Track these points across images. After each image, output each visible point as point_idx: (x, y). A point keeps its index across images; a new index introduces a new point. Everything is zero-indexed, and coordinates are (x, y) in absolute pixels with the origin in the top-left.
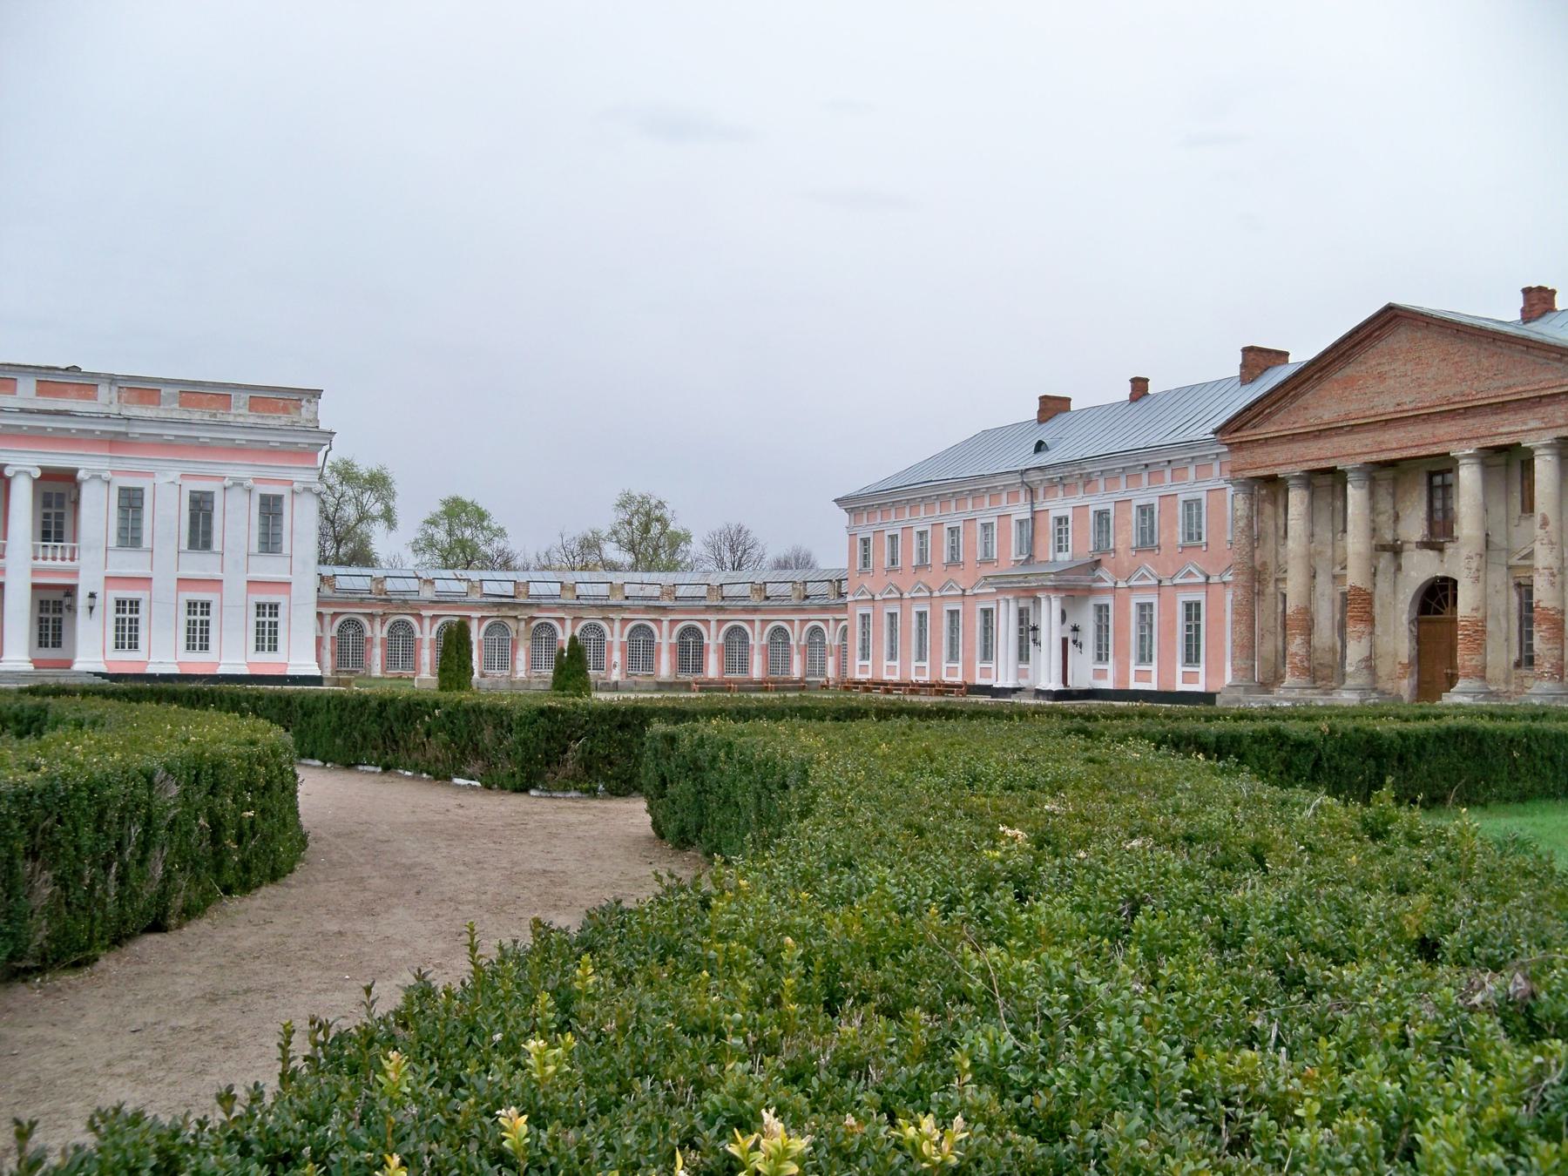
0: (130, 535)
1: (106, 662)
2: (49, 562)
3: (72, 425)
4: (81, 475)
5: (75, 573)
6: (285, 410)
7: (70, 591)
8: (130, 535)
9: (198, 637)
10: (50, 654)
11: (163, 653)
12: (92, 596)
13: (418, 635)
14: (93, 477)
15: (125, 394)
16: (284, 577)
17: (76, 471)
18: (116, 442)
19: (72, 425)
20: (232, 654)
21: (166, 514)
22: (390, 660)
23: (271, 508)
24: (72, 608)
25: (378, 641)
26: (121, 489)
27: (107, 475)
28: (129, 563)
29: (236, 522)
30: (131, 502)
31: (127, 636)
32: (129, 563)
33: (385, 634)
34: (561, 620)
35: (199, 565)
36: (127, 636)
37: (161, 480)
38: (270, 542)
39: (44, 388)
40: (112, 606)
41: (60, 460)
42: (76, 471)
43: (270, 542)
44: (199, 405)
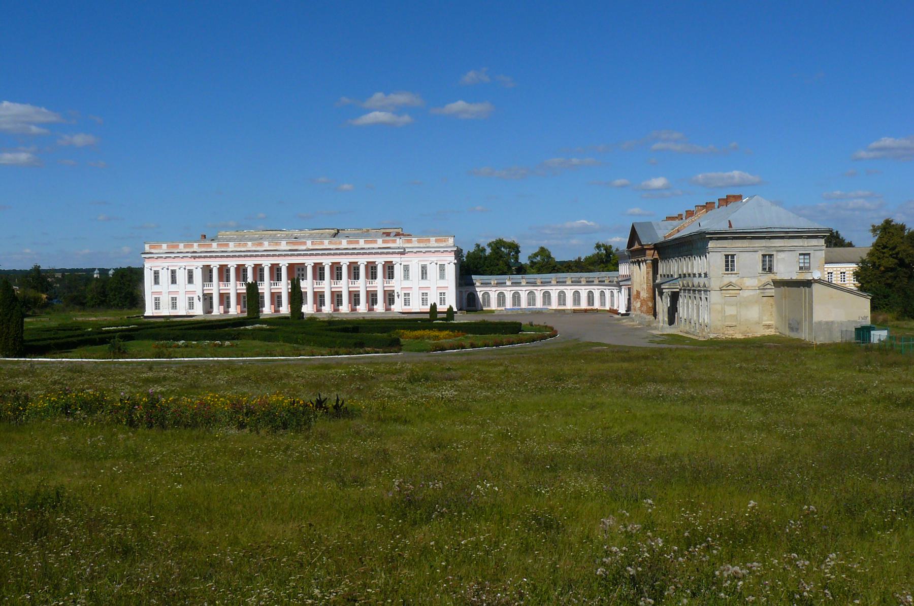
0: (406, 276)
3: (391, 251)
7: (393, 291)
8: (406, 276)
19: (391, 251)
21: (415, 271)
23: (442, 268)
28: (406, 284)
29: (433, 271)
30: (406, 269)
31: (407, 302)
35: (424, 283)
36: (407, 302)
38: (442, 276)
41: (388, 258)
43: (442, 276)
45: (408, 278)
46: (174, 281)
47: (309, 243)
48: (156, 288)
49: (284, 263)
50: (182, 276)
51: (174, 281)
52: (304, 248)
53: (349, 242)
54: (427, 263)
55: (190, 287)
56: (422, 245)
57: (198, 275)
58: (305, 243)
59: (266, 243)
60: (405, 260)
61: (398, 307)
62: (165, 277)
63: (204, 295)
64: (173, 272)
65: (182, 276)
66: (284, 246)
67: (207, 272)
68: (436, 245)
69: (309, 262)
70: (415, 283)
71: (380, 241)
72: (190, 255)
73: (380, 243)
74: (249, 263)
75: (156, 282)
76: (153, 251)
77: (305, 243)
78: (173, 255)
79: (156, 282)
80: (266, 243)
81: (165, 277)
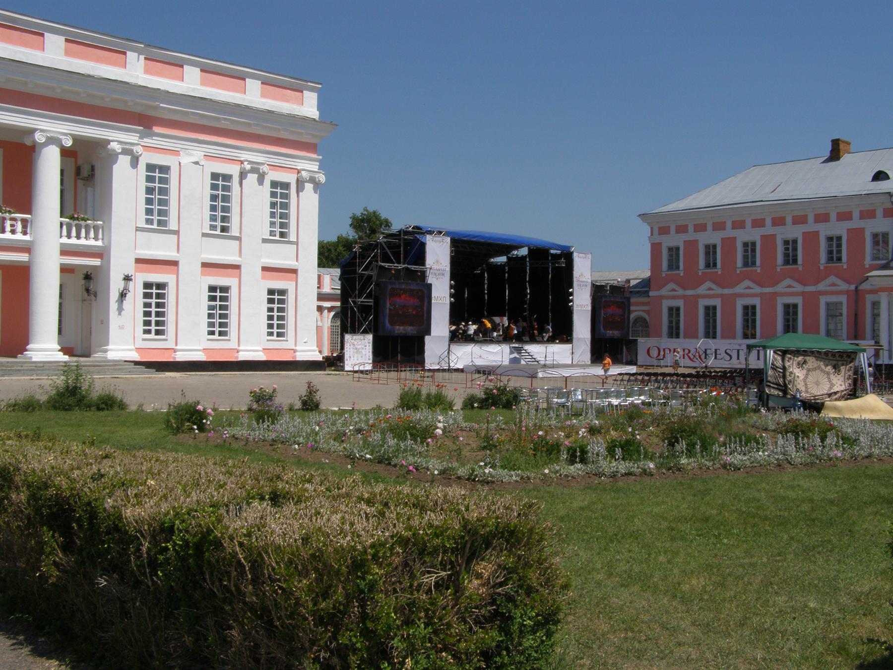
1: (138, 350)
5: (101, 253)
12: (127, 278)
14: (125, 152)
17: (108, 142)
27: (138, 149)
29: (252, 204)
30: (158, 180)
32: (159, 247)
40: (140, 291)
42: (108, 142)
54: (234, 170)
60: (153, 148)
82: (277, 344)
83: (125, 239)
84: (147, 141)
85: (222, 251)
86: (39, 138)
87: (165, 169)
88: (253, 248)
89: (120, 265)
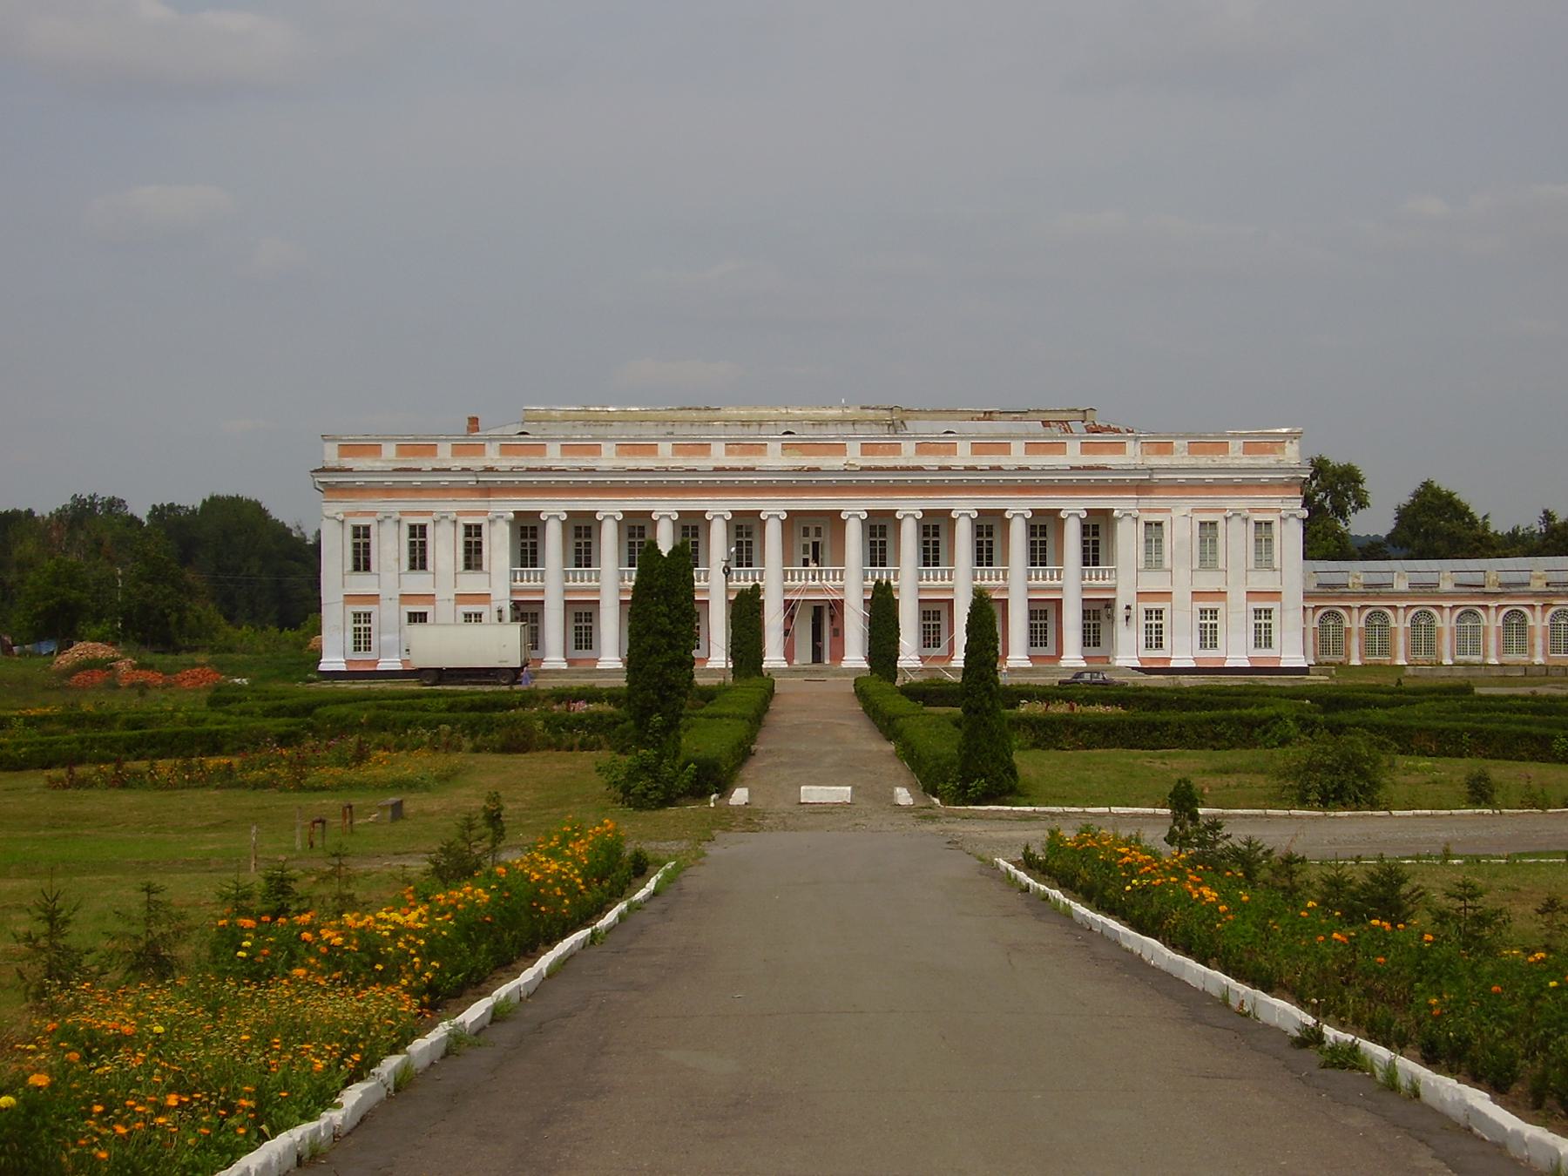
2: (1101, 582)
4: (1116, 513)
5: (1114, 590)
6: (1272, 452)
7: (1109, 604)
9: (1208, 636)
10: (1093, 651)
11: (1182, 652)
12: (1128, 607)
13: (1393, 625)
15: (1145, 447)
16: (1277, 588)
18: (1142, 487)
20: (1236, 651)
22: (1368, 648)
24: (1111, 617)
25: (1355, 631)
26: (1147, 524)
29: (1236, 541)
31: (1155, 638)
32: (1153, 582)
33: (1363, 625)
34: (1532, 607)
36: (1155, 638)
37: (1176, 514)
39: (1086, 448)
44: (1204, 452)
45: (1159, 565)
46: (418, 560)
47: (854, 449)
48: (362, 584)
49: (773, 509)
50: (445, 548)
51: (418, 560)
52: (836, 462)
53: (978, 449)
54: (1217, 517)
55: (472, 583)
56: (1203, 461)
57: (499, 545)
58: (840, 449)
59: (718, 449)
61: (1127, 652)
62: (389, 547)
63: (516, 605)
64: (418, 532)
65: (445, 548)
66: (774, 459)
67: (528, 533)
68: (1246, 461)
69: (855, 509)
70: (1181, 578)
71: (1073, 447)
72: (471, 479)
73: (1073, 455)
74: (665, 510)
75: (362, 561)
76: (348, 462)
77: (840, 449)
78: (417, 480)
79: (362, 561)
80: (718, 449)
81: (389, 547)
82: (1264, 652)
83: (1126, 576)
84: (1144, 504)
85: (1208, 582)
86: (1063, 515)
87: (1159, 524)
88: (1237, 572)
89: (1123, 598)
